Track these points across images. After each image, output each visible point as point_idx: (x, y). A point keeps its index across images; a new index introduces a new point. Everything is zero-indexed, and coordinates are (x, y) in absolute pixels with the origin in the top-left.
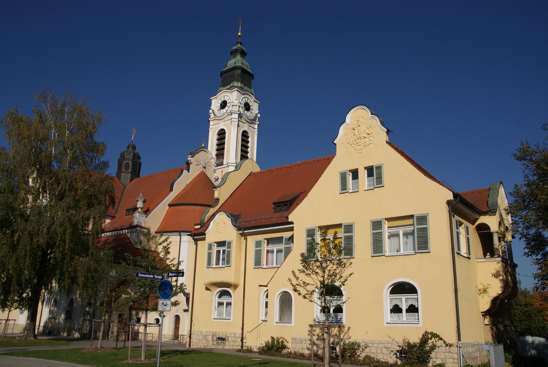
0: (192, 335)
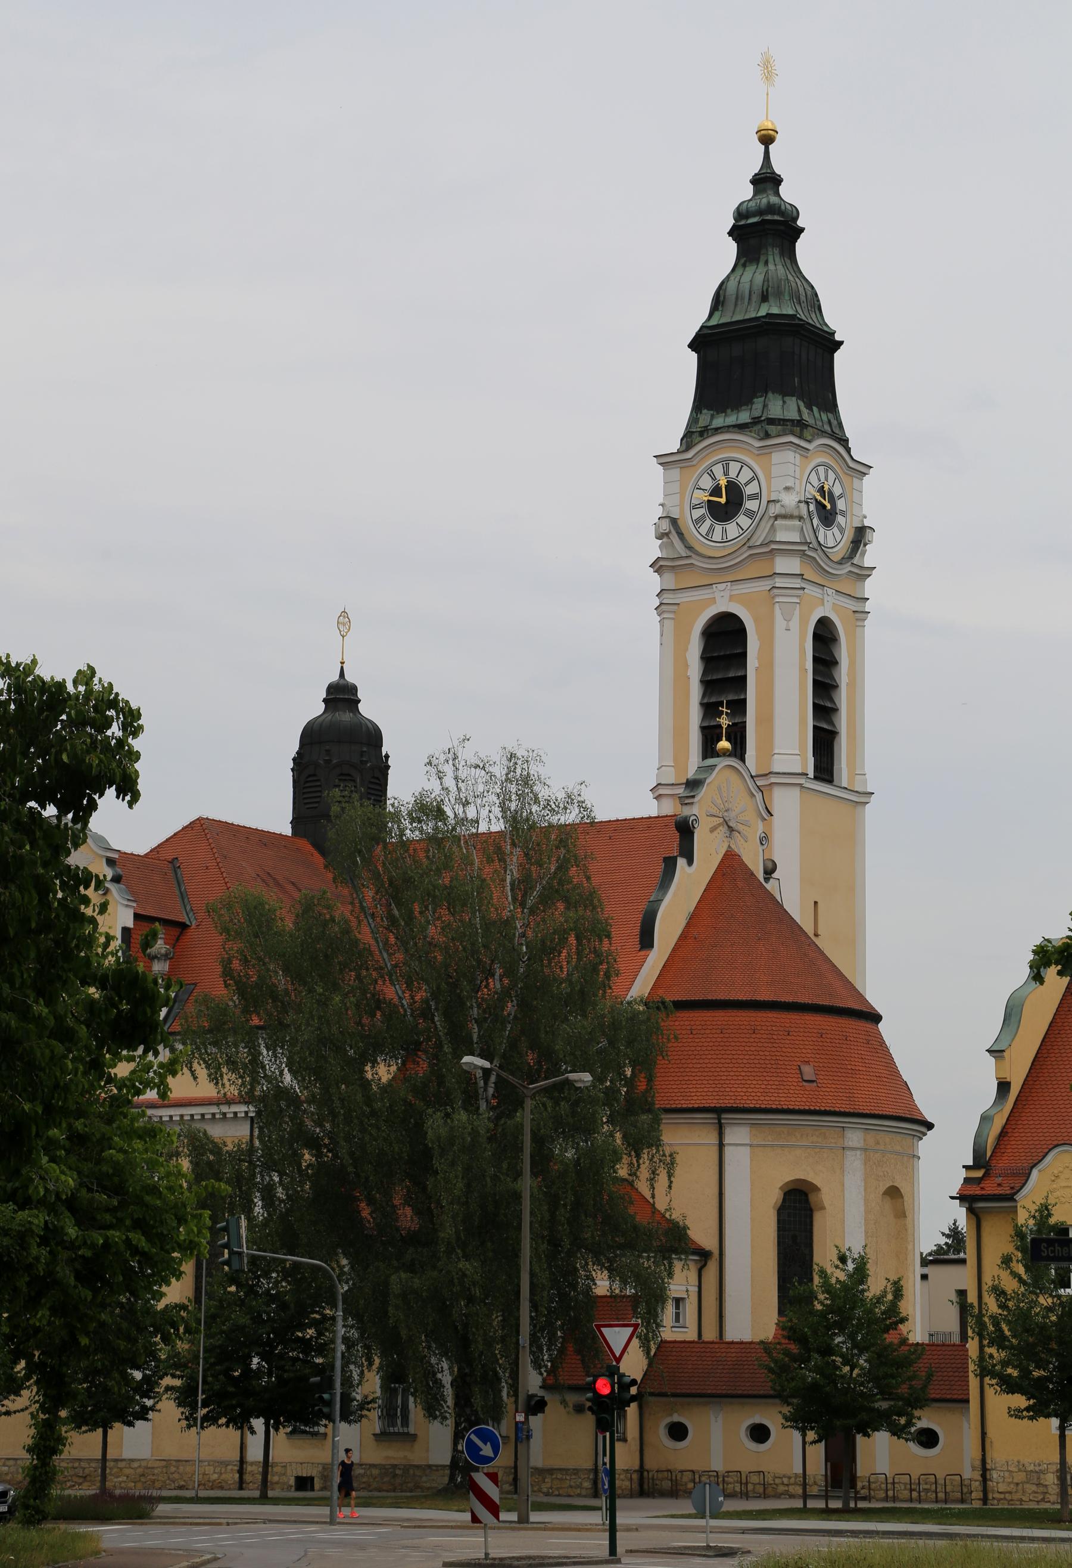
0: (988, 1472)
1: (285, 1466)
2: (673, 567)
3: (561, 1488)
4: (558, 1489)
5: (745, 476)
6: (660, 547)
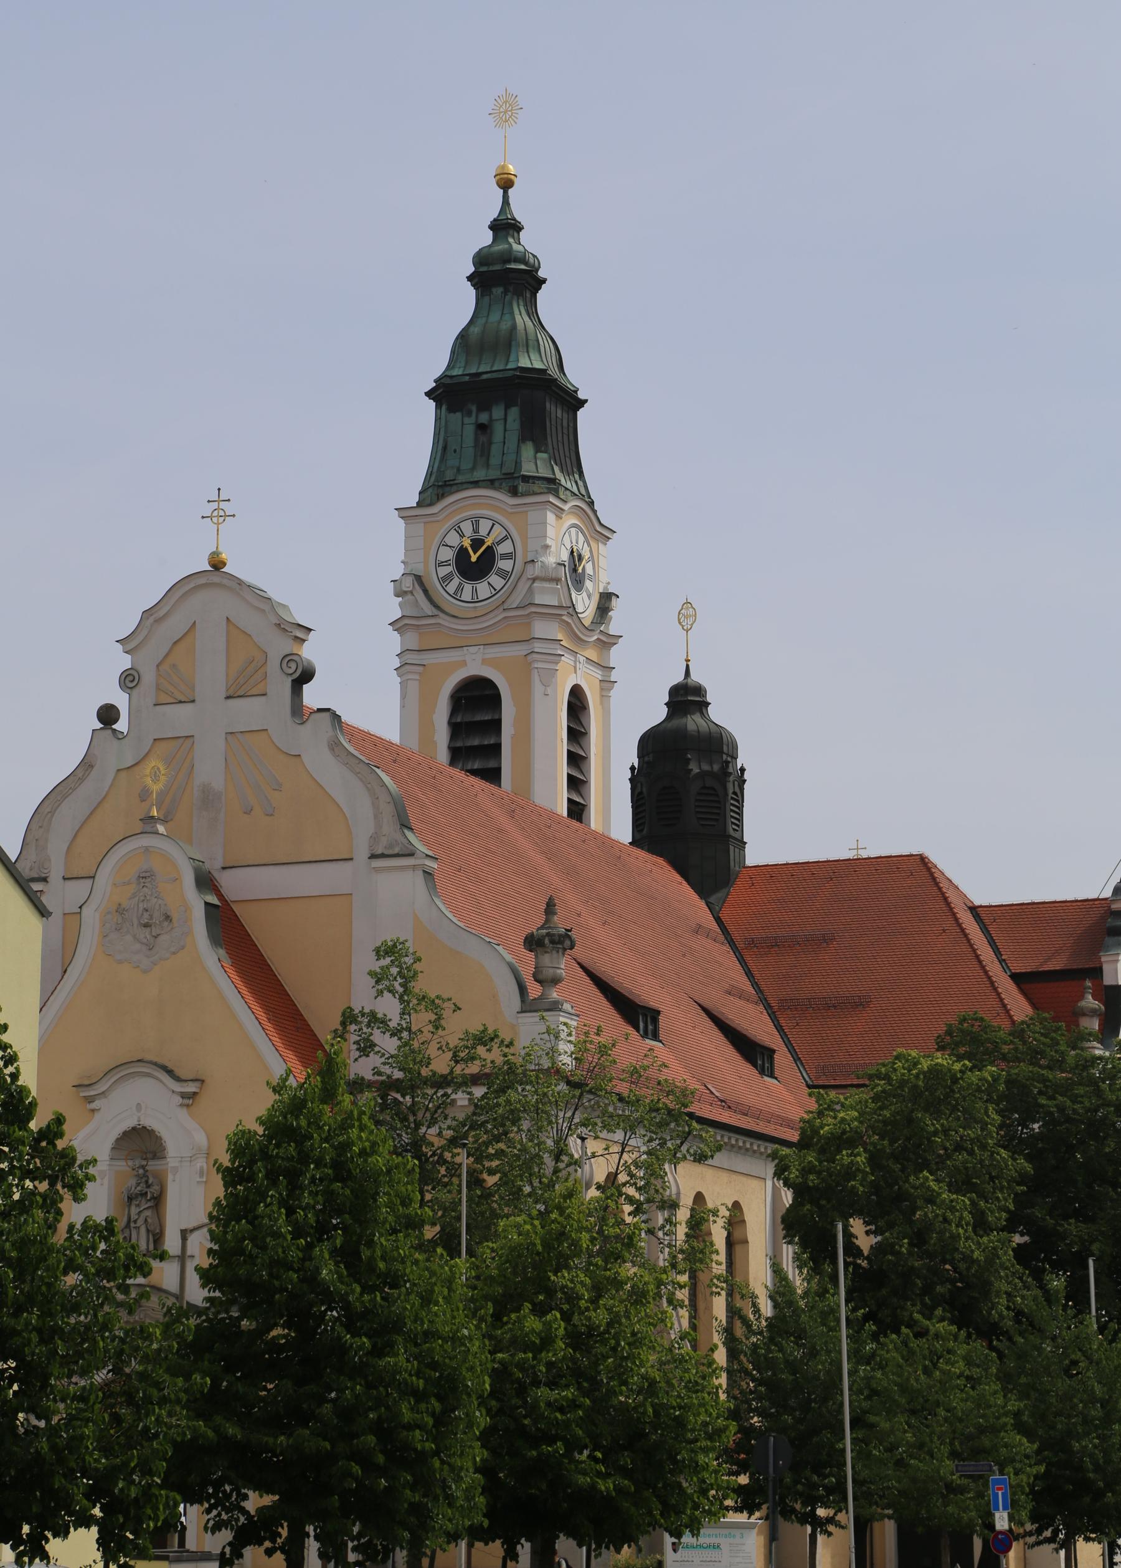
6: (400, 604)
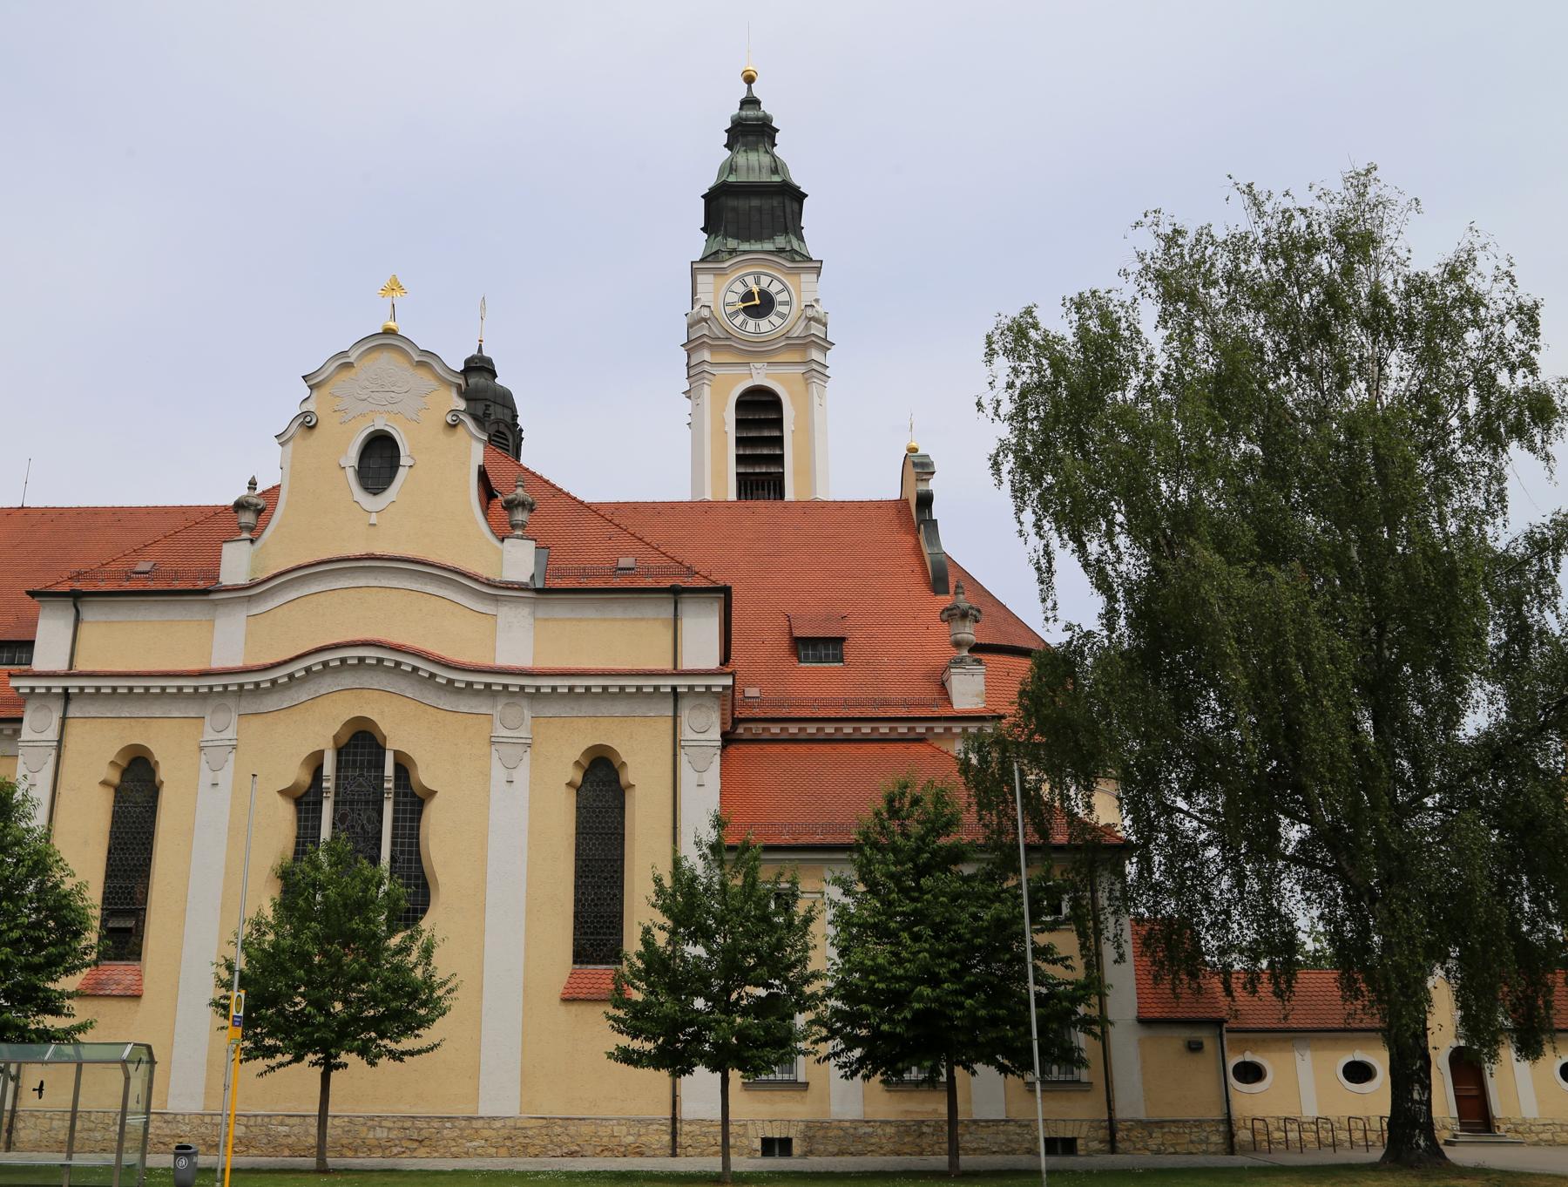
1: (745, 1125)
2: (711, 345)
3: (1178, 1144)
4: (1173, 1145)
5: (774, 288)
